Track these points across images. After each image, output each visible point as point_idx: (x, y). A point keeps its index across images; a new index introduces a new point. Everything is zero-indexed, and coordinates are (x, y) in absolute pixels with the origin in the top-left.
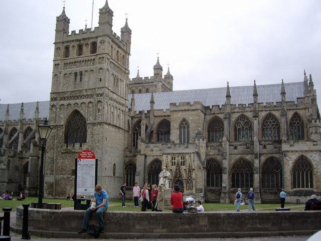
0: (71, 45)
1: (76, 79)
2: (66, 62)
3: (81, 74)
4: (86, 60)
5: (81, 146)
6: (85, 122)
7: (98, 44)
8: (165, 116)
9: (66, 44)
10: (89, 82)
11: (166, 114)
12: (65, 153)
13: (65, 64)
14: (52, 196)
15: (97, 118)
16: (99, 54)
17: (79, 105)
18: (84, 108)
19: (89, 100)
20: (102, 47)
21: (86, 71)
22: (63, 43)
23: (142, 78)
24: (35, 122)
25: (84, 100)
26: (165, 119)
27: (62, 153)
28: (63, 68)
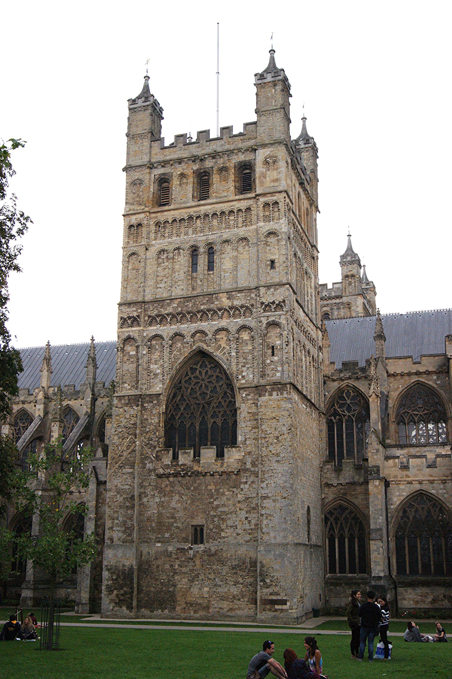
0: (179, 169)
1: (194, 265)
2: (161, 217)
3: (211, 251)
4: (223, 213)
5: (220, 455)
6: (230, 386)
7: (259, 169)
8: (418, 373)
9: (159, 171)
10: (235, 269)
11: (422, 369)
12: (168, 476)
13: (158, 224)
14: (130, 608)
15: (268, 372)
16: (264, 195)
17: (210, 336)
18: (223, 346)
19: (240, 321)
20: (272, 174)
21: (227, 241)
22: (151, 166)
23: (326, 285)
24: (41, 396)
25: (224, 323)
26: (418, 383)
27: (160, 476)
28: (152, 236)
